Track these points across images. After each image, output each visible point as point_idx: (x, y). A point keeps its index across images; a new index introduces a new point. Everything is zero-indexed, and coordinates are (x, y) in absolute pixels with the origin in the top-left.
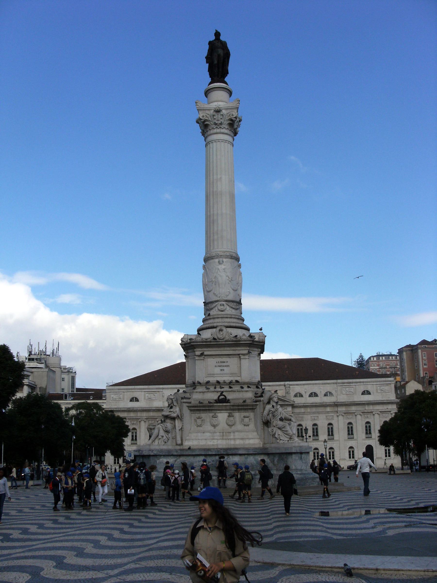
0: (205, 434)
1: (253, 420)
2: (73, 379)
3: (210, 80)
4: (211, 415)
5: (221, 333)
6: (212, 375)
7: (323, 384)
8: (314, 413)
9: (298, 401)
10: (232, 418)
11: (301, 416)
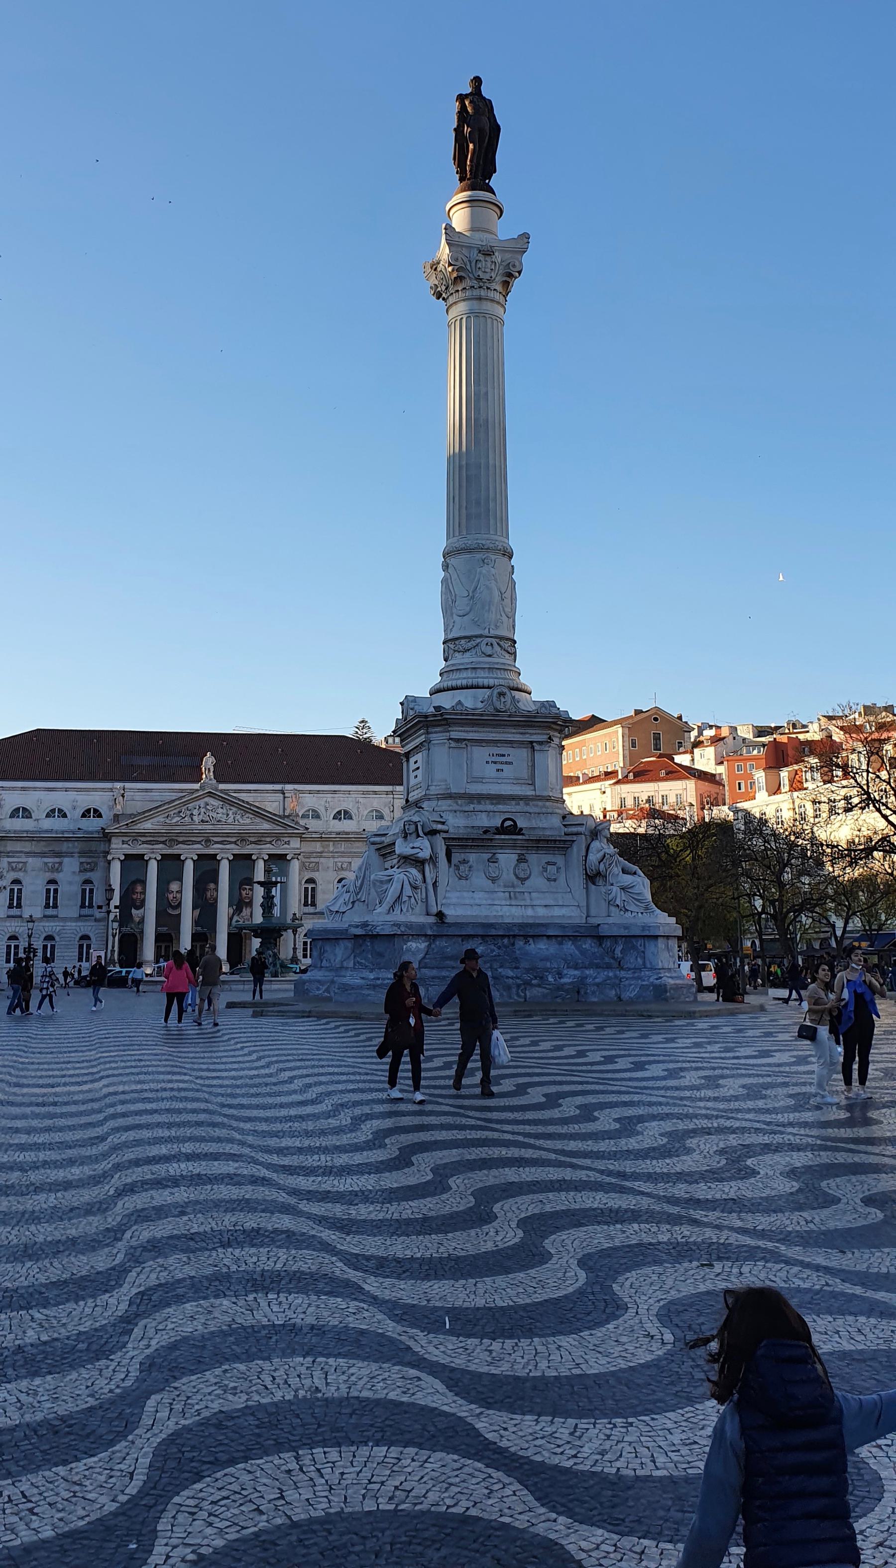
0: (476, 895)
1: (563, 869)
4: (486, 856)
5: (503, 700)
6: (480, 780)
7: (364, 793)
8: (343, 854)
10: (523, 865)
11: (312, 860)
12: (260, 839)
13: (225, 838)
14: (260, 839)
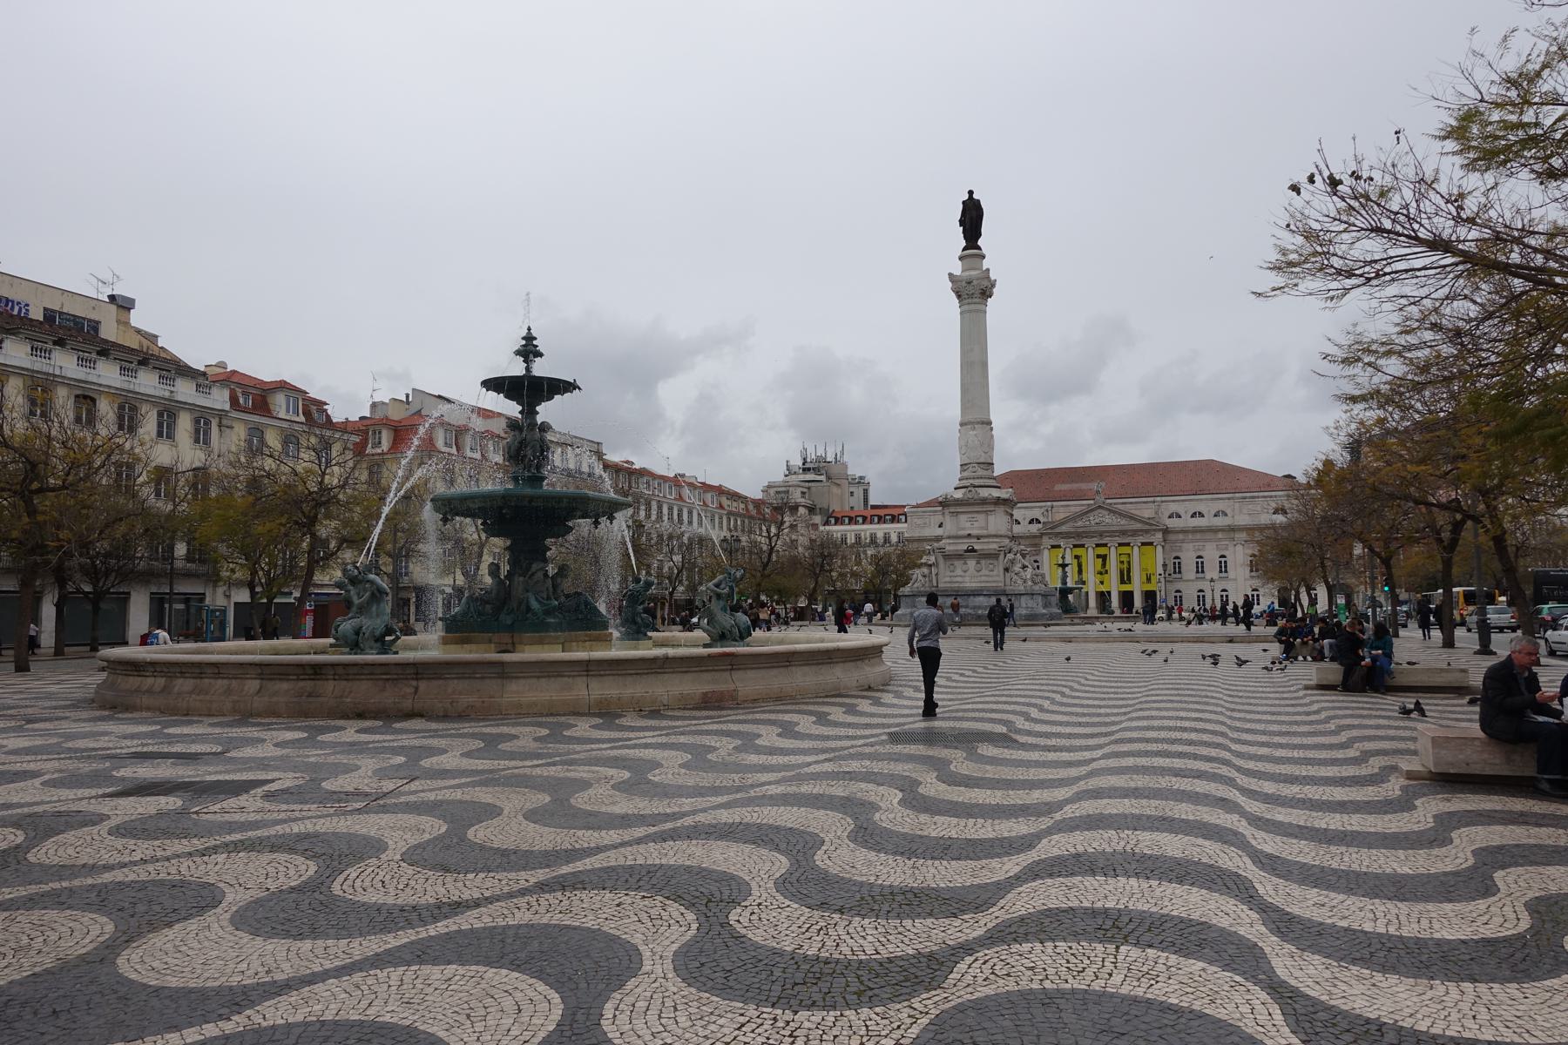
2: (866, 492)
3: (964, 243)
9: (1173, 523)
12: (1135, 533)
13: (1112, 534)
14: (1135, 533)
